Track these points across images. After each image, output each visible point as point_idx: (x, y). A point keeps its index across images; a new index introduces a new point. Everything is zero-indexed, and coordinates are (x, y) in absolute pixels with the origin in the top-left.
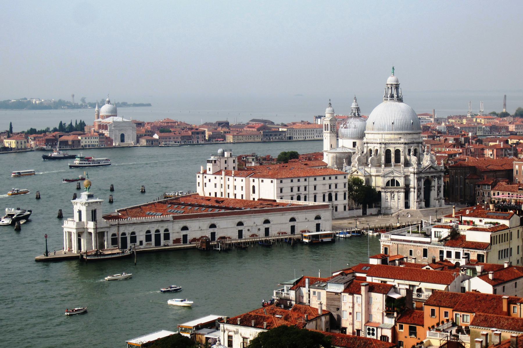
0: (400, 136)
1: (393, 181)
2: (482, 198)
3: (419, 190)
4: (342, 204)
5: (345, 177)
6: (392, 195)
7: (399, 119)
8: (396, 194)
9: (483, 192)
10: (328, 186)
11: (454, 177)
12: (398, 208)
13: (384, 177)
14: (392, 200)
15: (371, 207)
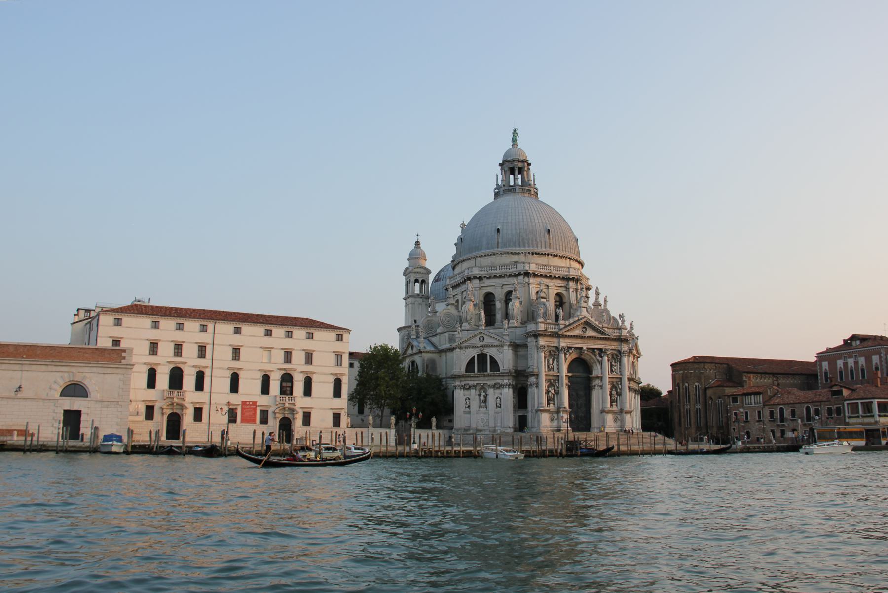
0: (516, 258)
1: (482, 357)
2: (743, 427)
3: (554, 382)
4: (328, 409)
5: (340, 338)
6: (480, 395)
7: (513, 221)
8: (491, 391)
9: (746, 413)
10: (280, 356)
11: (681, 385)
12: (495, 431)
13: (460, 348)
14: (483, 410)
15: (424, 424)
